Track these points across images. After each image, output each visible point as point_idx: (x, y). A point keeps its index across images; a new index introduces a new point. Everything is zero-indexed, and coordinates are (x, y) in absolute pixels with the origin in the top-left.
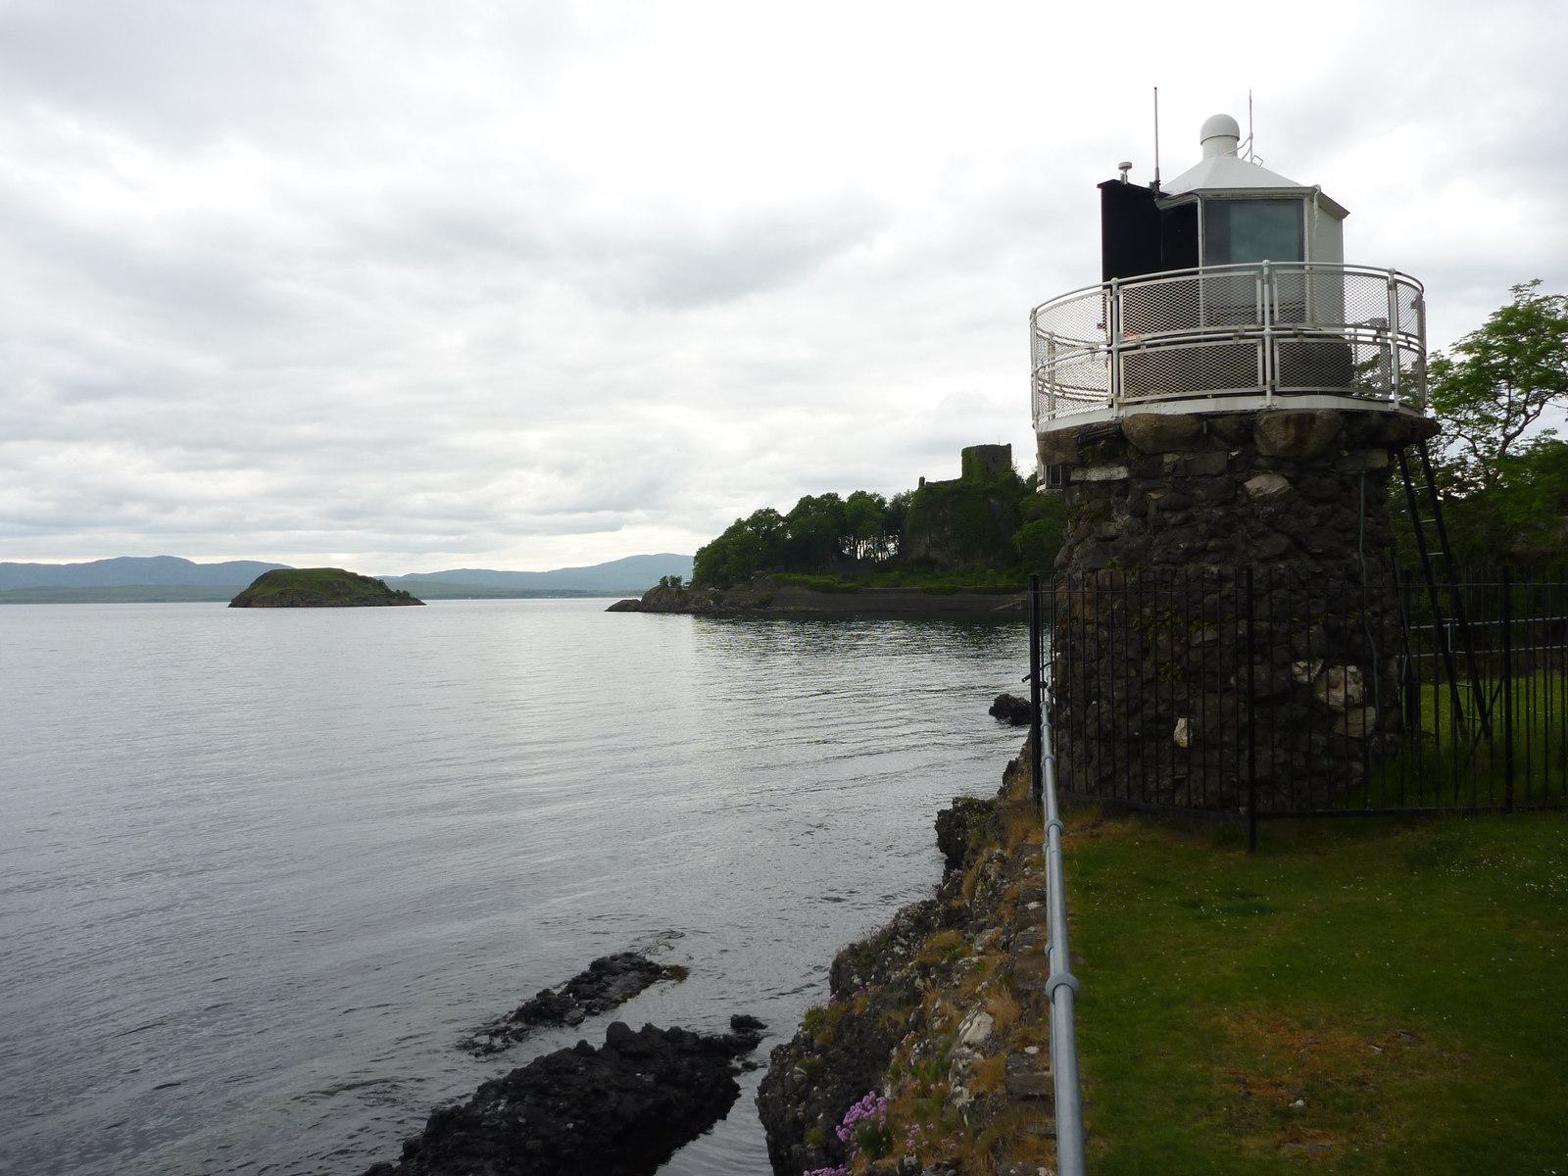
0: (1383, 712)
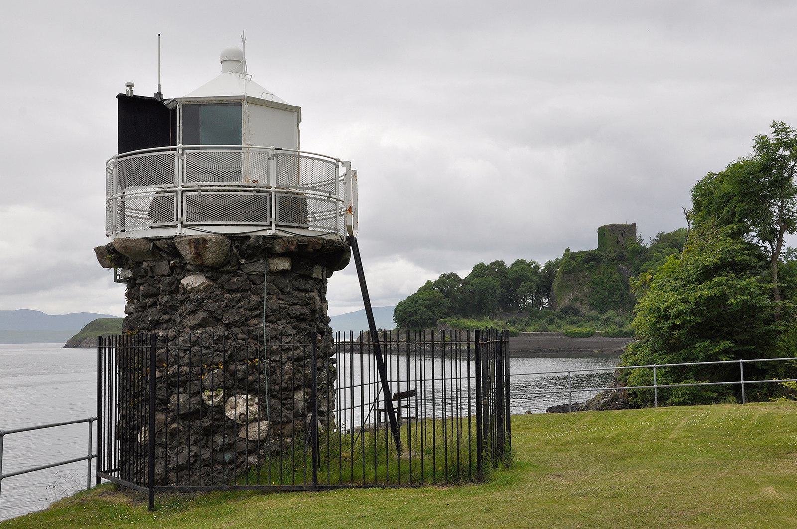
0: (273, 425)
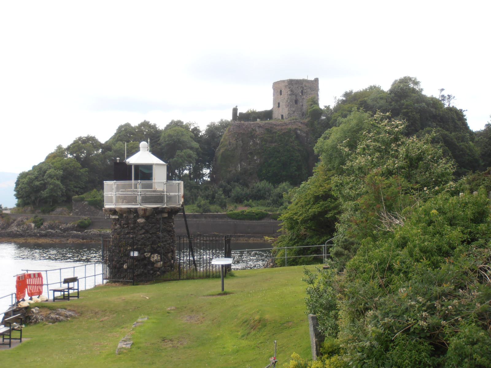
0: (164, 263)
